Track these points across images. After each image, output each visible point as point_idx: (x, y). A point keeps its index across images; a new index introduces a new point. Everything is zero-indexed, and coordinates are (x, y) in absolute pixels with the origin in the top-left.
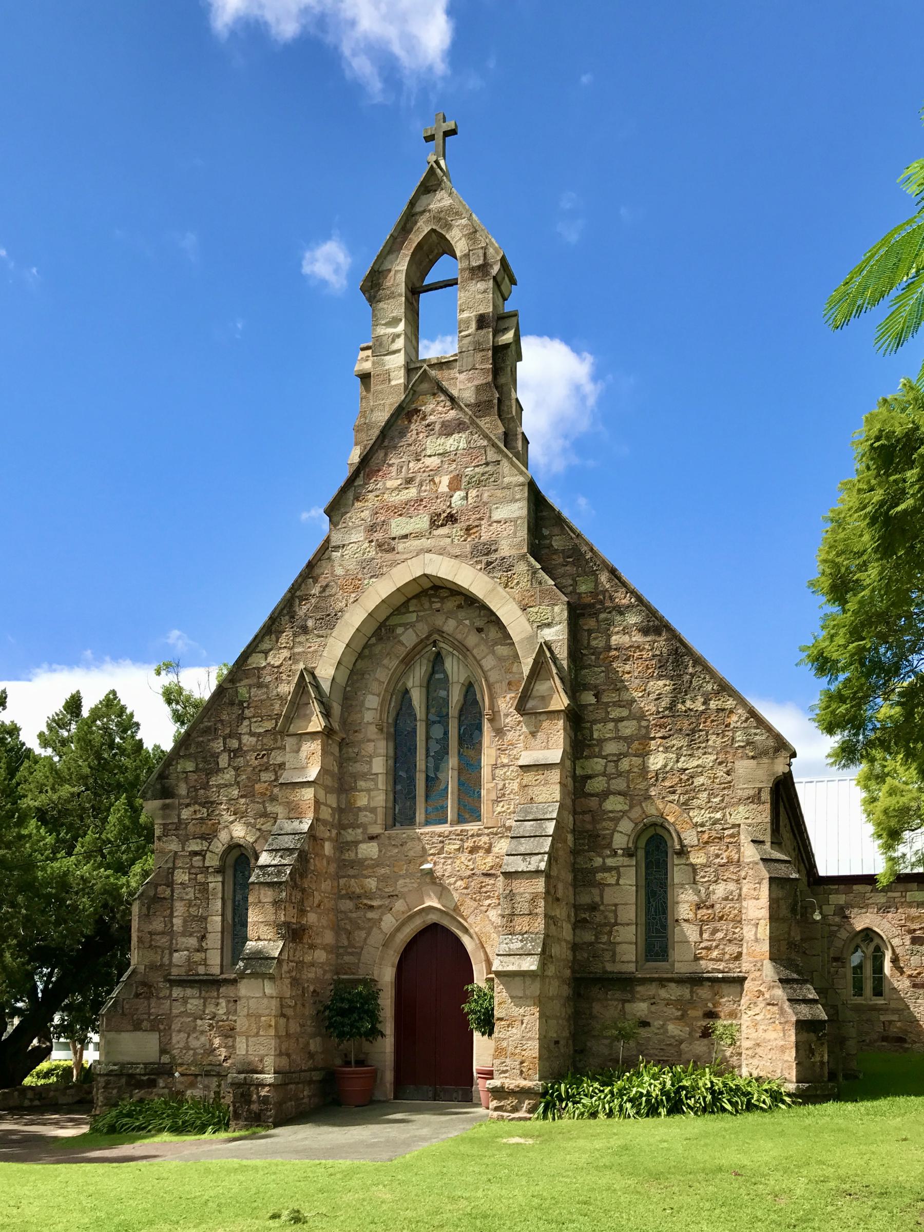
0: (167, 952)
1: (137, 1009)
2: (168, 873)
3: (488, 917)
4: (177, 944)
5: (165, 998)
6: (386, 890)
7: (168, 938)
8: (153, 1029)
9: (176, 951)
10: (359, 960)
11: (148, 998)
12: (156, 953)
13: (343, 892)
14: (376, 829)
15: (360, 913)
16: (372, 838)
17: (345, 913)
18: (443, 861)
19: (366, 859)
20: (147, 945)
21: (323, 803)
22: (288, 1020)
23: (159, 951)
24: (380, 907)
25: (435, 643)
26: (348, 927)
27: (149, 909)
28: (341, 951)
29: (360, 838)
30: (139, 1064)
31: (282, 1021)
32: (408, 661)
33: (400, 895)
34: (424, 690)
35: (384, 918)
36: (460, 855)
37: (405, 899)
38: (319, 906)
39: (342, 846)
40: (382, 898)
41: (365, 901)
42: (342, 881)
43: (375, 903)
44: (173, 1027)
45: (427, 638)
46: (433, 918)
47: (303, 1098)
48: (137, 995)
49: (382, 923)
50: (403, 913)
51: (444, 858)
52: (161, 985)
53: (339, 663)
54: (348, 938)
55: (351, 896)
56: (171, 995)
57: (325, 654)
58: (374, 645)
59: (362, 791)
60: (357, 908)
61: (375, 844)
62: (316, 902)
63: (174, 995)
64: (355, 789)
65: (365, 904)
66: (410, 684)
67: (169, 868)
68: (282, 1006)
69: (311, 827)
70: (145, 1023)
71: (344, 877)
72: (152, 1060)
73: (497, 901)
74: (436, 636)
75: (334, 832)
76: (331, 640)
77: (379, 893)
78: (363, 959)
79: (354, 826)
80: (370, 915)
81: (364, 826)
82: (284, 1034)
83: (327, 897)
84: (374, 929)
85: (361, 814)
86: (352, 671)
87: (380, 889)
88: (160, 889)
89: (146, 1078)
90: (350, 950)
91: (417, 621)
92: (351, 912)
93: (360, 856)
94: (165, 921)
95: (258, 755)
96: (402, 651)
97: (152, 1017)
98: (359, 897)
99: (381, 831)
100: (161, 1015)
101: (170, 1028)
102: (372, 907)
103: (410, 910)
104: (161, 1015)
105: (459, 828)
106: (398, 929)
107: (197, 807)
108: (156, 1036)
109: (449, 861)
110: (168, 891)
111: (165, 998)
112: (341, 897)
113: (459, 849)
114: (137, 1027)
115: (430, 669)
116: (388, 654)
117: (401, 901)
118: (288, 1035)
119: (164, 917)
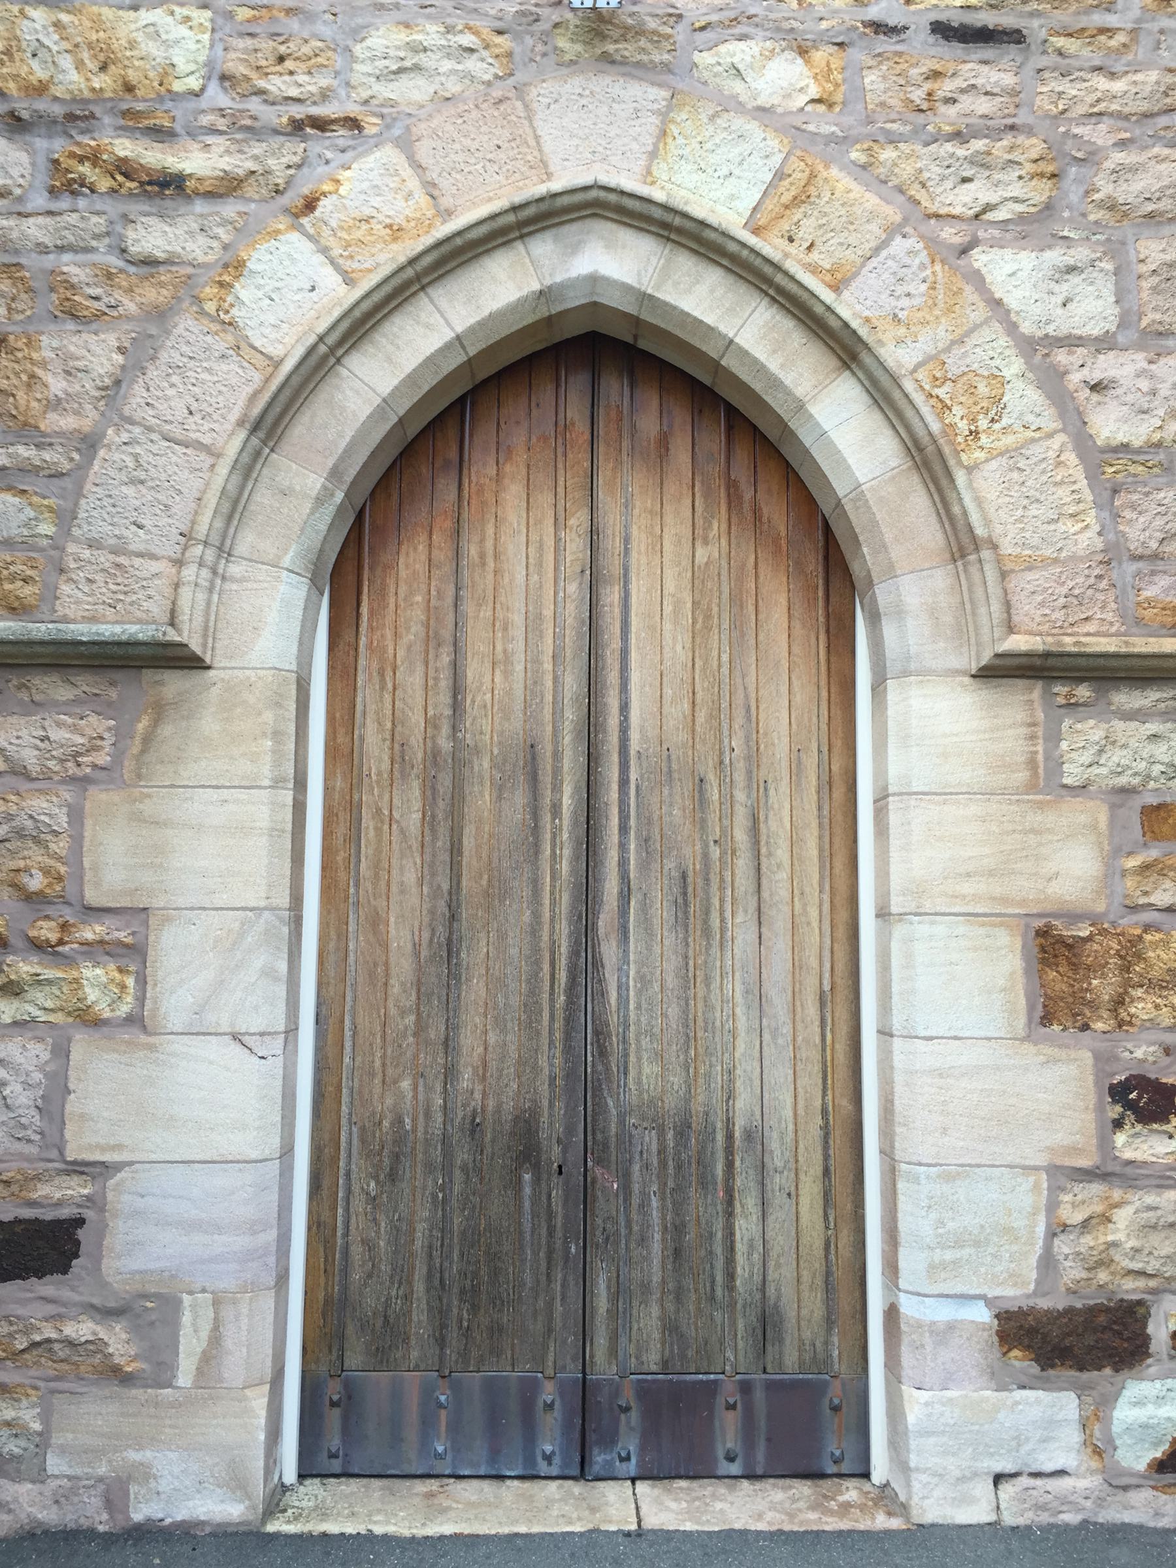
3: (978, 280)
6: (276, 85)
10: (66, 518)
15: (86, 218)
24: (228, 187)
33: (372, 125)
35: (260, 258)
37: (406, 145)
41: (125, 148)
43: (197, 161)
46: (614, 263)
49: (244, 291)
50: (396, 232)
60: (65, 185)
65: (125, 168)
73: (1039, 192)
77: (216, 96)
78: (94, 517)
80: (153, 235)
84: (186, 325)
98: (77, 117)
102: (168, 187)
103: (449, 214)
106: (359, 326)
117: (388, 154)
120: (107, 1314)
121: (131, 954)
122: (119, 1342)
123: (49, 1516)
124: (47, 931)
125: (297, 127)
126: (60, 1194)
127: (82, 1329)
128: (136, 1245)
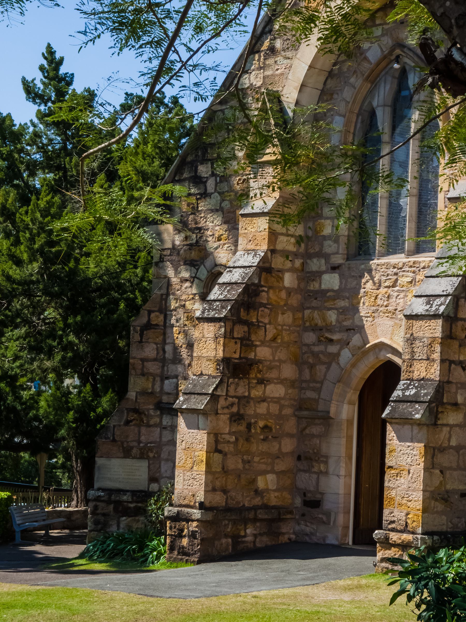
0: (158, 379)
1: (127, 436)
2: (162, 299)
4: (168, 371)
5: (155, 425)
6: (345, 323)
7: (161, 364)
8: (142, 456)
9: (167, 378)
10: (319, 394)
11: (139, 426)
12: (148, 379)
13: (308, 324)
14: (338, 260)
15: (321, 348)
16: (334, 268)
17: (308, 345)
18: (396, 294)
19: (328, 291)
20: (139, 372)
21: (282, 234)
22: (225, 455)
23: (151, 378)
24: (339, 341)
25: (397, 60)
26: (311, 360)
27: (141, 335)
28: (304, 385)
29: (324, 268)
30: (124, 492)
31: (217, 457)
32: (373, 79)
34: (388, 110)
36: (412, 288)
38: (274, 339)
39: (307, 276)
40: (340, 331)
42: (307, 312)
43: (335, 337)
44: (162, 456)
45: (391, 53)
47: (245, 536)
48: (128, 423)
51: (398, 291)
52: (152, 412)
53: (303, 86)
54: (311, 372)
55: (315, 329)
56: (161, 421)
57: (290, 77)
58: (344, 61)
59: (327, 218)
60: (320, 341)
61: (337, 276)
62: (270, 336)
63: (164, 423)
64: (320, 216)
65: (326, 338)
66: (375, 104)
67: (162, 295)
68: (217, 442)
69: (264, 260)
70: (134, 451)
71: (308, 308)
72: (141, 488)
74: (398, 52)
75: (298, 263)
76: (295, 62)
79: (320, 255)
81: (327, 257)
82: (219, 470)
83: (286, 330)
85: (327, 243)
86: (322, 91)
87: (340, 323)
88: (153, 315)
89: (132, 505)
90: (311, 385)
91: (383, 35)
92: (314, 345)
93: (323, 287)
94: (157, 349)
95: (240, 180)
96: (366, 67)
97: (141, 445)
99: (341, 261)
100: (151, 443)
101: (159, 456)
102: (331, 341)
104: (151, 443)
105: (412, 259)
107: (189, 233)
108: (144, 464)
109: (402, 295)
110: (162, 317)
111: (155, 425)
112: (306, 329)
113: (411, 282)
114: (127, 453)
115: (395, 86)
116: (355, 72)
118: (225, 471)
119: (156, 344)
120: (323, 514)
121: (326, 463)
122: (325, 519)
123: (319, 542)
124: (317, 458)
125: (347, 330)
126: (318, 496)
127: (320, 516)
128: (327, 505)
